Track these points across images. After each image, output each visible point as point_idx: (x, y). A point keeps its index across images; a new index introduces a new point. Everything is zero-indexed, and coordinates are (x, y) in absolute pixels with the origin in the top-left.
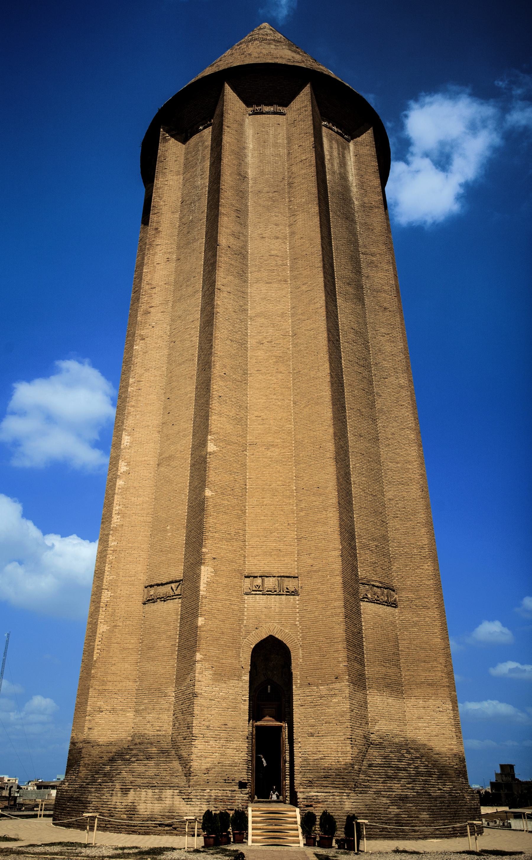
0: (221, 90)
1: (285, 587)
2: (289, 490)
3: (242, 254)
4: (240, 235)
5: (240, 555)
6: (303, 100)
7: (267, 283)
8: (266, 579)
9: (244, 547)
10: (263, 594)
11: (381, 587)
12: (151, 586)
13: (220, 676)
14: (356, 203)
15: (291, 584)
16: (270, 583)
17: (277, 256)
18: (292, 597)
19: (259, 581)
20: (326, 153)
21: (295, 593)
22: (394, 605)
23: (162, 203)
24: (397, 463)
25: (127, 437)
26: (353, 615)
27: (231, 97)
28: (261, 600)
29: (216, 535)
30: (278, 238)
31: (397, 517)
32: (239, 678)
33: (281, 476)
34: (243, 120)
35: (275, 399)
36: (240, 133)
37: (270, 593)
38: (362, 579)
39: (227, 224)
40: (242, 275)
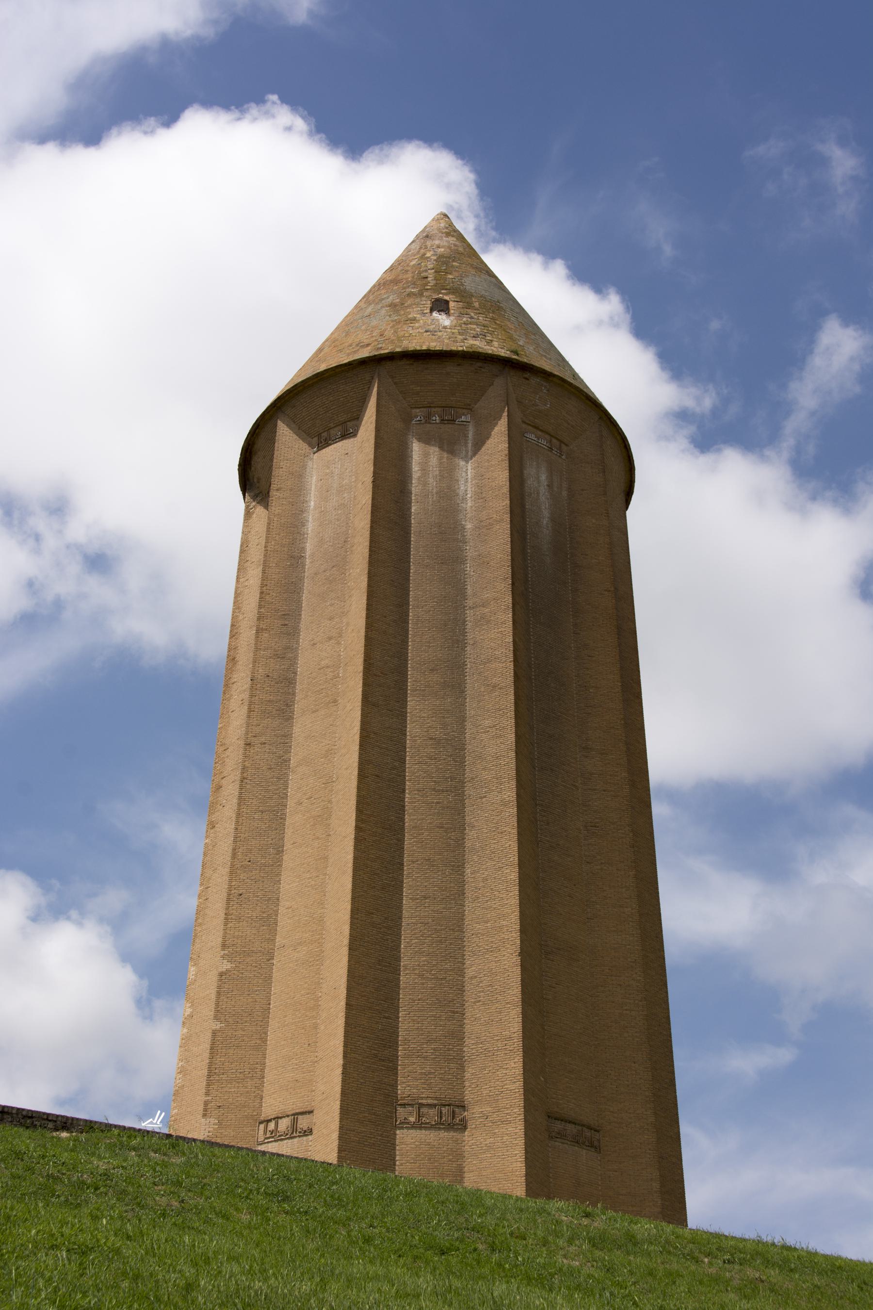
2: (313, 999)
5: (255, 1097)
7: (313, 712)
8: (280, 1121)
9: (260, 1087)
10: (275, 1141)
11: (435, 1106)
14: (469, 526)
15: (303, 1122)
17: (328, 667)
18: (305, 1138)
19: (272, 1126)
20: (415, 468)
21: (308, 1132)
23: (241, 617)
24: (487, 922)
25: (193, 969)
29: (224, 1077)
30: (330, 638)
31: (479, 1001)
33: (306, 983)
34: (304, 467)
35: (309, 878)
38: (403, 1098)
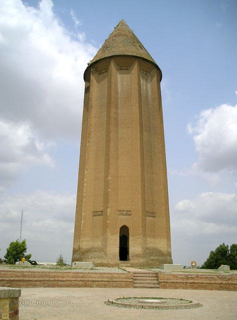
0: (110, 63)
1: (128, 213)
3: (117, 119)
4: (116, 113)
6: (135, 68)
12: (95, 212)
13: (113, 234)
15: (129, 213)
16: (124, 213)
21: (130, 215)
22: (154, 217)
26: (144, 220)
27: (113, 66)
28: (122, 217)
32: (117, 234)
36: (116, 77)
37: (125, 215)
39: (113, 110)
40: (117, 126)
